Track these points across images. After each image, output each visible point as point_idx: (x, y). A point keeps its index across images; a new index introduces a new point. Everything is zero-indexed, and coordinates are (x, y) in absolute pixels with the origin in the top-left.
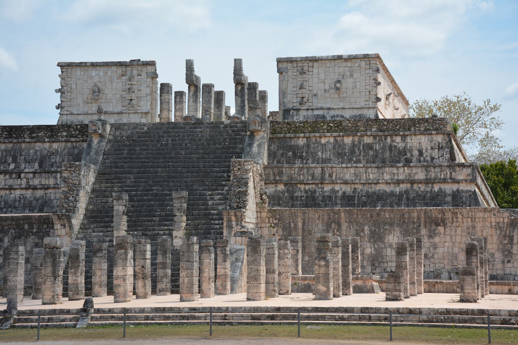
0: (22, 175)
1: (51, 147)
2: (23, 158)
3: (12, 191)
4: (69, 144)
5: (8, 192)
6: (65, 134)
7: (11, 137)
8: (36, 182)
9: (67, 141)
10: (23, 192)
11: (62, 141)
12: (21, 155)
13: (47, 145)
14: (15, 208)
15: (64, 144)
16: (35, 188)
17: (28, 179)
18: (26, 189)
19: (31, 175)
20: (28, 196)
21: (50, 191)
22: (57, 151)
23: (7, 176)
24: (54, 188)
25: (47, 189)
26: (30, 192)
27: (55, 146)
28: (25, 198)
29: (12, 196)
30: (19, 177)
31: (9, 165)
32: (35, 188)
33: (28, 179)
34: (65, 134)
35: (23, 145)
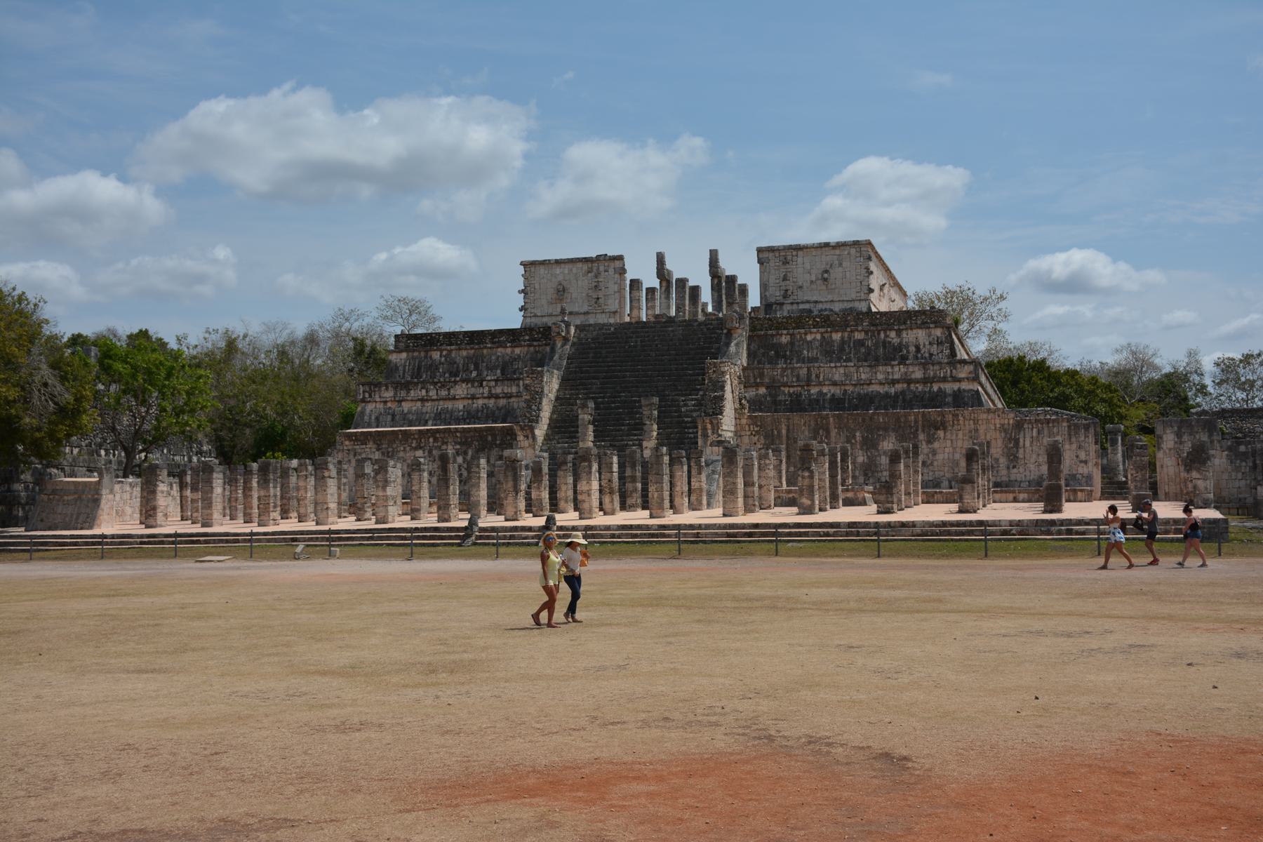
1: (513, 352)
4: (532, 349)
8: (498, 390)
9: (529, 346)
10: (486, 401)
13: (509, 350)
16: (497, 397)
18: (489, 398)
26: (492, 401)
27: (517, 351)
28: (488, 408)
35: (485, 351)
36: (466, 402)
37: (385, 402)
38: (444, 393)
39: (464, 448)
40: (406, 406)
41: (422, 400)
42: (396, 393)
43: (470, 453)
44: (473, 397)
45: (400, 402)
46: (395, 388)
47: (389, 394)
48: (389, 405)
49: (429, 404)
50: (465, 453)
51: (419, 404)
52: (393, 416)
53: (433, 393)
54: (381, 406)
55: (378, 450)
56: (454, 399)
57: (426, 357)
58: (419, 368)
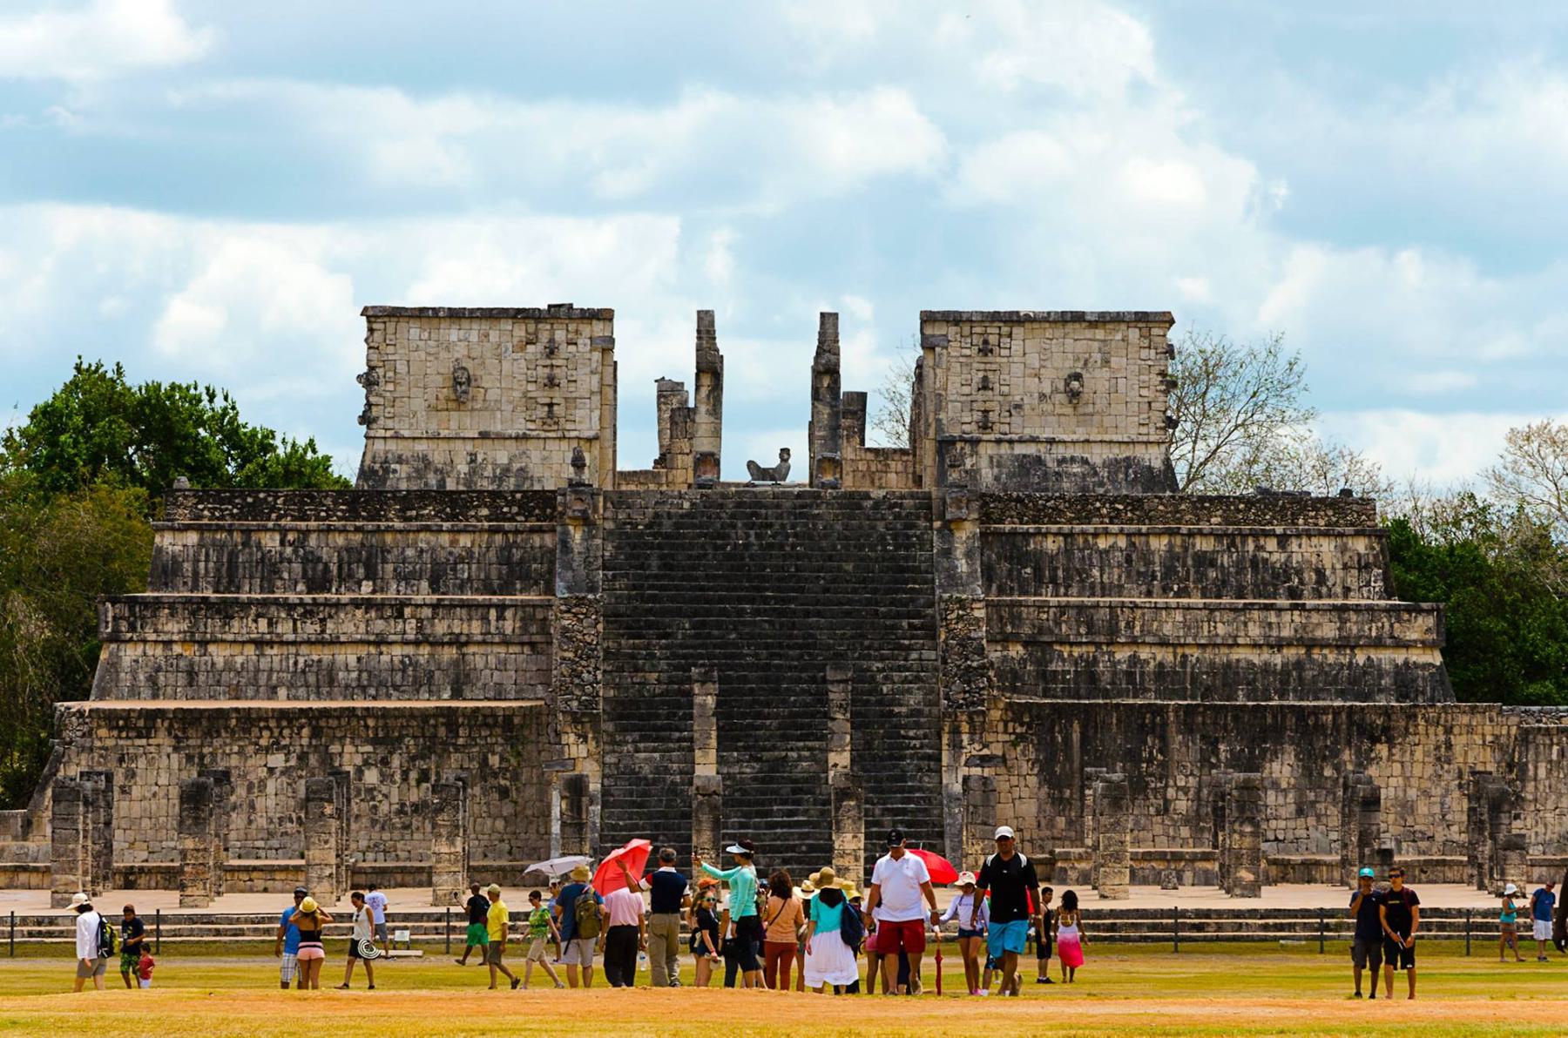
1: (454, 543)
2: (390, 567)
3: (384, 649)
4: (498, 538)
5: (372, 650)
6: (485, 512)
7: (357, 517)
9: (493, 531)
10: (410, 650)
11: (482, 531)
12: (384, 561)
13: (445, 539)
14: (396, 688)
16: (437, 643)
18: (417, 643)
20: (422, 660)
21: (471, 649)
22: (470, 551)
24: (484, 643)
25: (466, 644)
26: (425, 650)
27: (465, 540)
28: (415, 665)
29: (385, 658)
31: (359, 584)
32: (437, 643)
34: (485, 512)
35: (389, 538)
36: (363, 651)
37: (168, 644)
39: (382, 751)
40: (218, 654)
41: (259, 643)
43: (396, 761)
44: (381, 642)
45: (204, 643)
48: (177, 649)
50: (385, 762)
52: (191, 674)
55: (176, 749)
56: (335, 642)
57: (246, 544)
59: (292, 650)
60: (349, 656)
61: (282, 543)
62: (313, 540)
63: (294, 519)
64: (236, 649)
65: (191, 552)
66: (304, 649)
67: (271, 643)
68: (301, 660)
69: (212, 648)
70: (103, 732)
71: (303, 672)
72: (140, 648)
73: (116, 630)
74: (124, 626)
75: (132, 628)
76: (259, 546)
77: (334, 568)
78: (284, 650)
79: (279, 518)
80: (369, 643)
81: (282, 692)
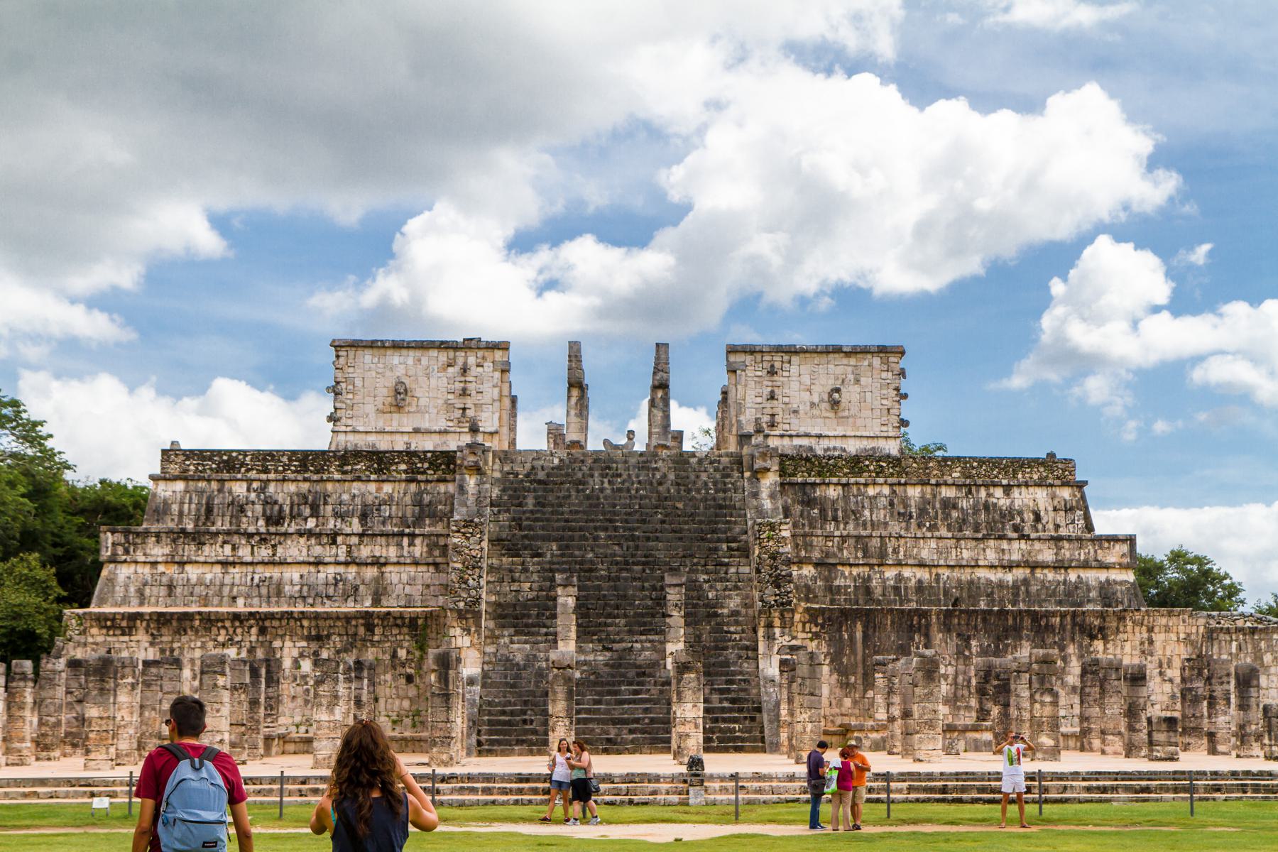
0: (340, 539)
2: (329, 508)
3: (321, 568)
4: (413, 487)
5: (312, 569)
6: (403, 467)
8: (365, 552)
9: (409, 481)
10: (341, 569)
13: (372, 487)
15: (403, 484)
17: (349, 546)
18: (347, 564)
19: (355, 540)
20: (350, 577)
22: (391, 497)
23: (313, 541)
24: (398, 563)
26: (353, 570)
27: (387, 488)
28: (344, 580)
29: (322, 576)
30: (334, 542)
31: (306, 520)
33: (349, 546)
34: (403, 467)
35: (329, 486)
36: (305, 570)
38: (264, 553)
40: (193, 572)
41: (225, 564)
42: (175, 550)
44: (318, 563)
45: (182, 564)
46: (174, 541)
47: (159, 551)
48: (161, 568)
49: (235, 571)
51: (218, 569)
53: (245, 553)
54: (147, 570)
56: (282, 563)
57: (220, 491)
58: (209, 510)
59: (250, 569)
60: (293, 574)
61: (248, 490)
62: (272, 488)
63: (259, 472)
64: (206, 569)
65: (179, 496)
66: (259, 569)
67: (233, 564)
68: (257, 577)
69: (188, 568)
70: (95, 631)
71: (258, 586)
72: (133, 567)
73: (114, 554)
74: (120, 550)
75: (127, 552)
76: (230, 492)
77: (287, 509)
78: (244, 569)
79: (248, 471)
80: (310, 563)
81: (240, 601)
